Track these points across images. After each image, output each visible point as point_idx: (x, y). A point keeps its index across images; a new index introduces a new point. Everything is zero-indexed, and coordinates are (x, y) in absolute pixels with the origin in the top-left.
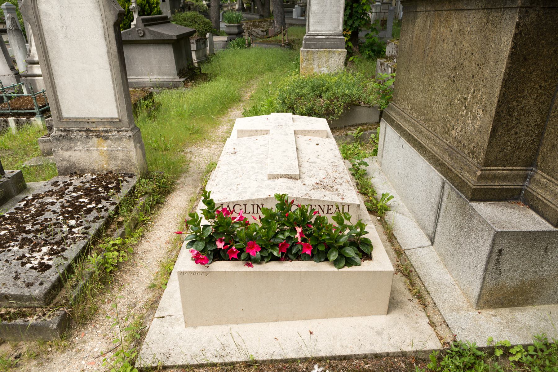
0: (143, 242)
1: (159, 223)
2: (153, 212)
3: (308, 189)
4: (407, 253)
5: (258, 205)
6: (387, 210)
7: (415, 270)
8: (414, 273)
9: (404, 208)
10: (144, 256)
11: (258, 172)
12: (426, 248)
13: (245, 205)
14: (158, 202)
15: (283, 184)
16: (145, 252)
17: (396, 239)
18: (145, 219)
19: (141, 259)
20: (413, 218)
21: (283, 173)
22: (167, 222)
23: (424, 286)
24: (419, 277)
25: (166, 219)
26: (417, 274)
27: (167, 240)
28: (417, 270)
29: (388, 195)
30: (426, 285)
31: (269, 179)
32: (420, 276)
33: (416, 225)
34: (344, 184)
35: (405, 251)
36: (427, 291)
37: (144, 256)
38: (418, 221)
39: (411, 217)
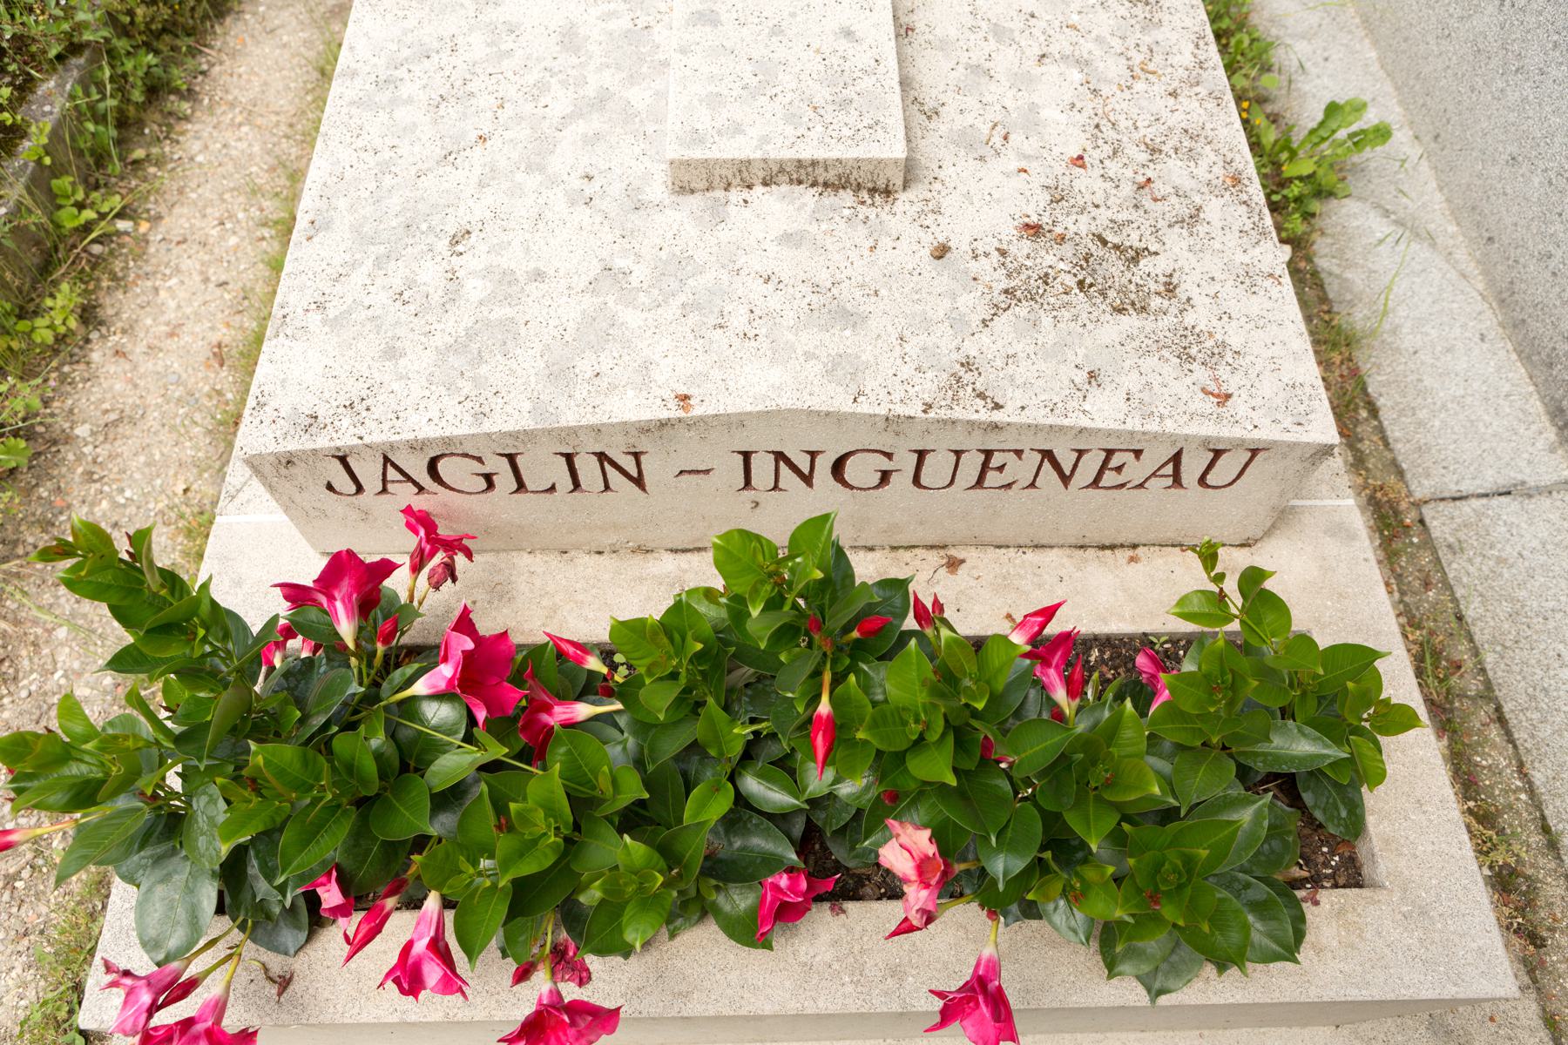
0: (95, 356)
1: (178, 221)
2: (139, 153)
3: (972, 304)
4: (1440, 523)
5: (602, 457)
6: (1331, 194)
7: (1476, 652)
8: (1474, 686)
9: (1426, 197)
10: (103, 452)
11: (602, 100)
12: (1545, 502)
13: (511, 458)
14: (155, 90)
15: (787, 263)
16: (108, 430)
17: (1374, 411)
18: (88, 214)
19: (89, 477)
20: (1472, 268)
21: (782, 151)
22: (215, 212)
23: (1531, 790)
24: (1501, 720)
25: (207, 192)
26: (1488, 692)
27: (215, 338)
28: (1489, 659)
29: (1359, 108)
30: (1538, 778)
31: (684, 189)
32: (1507, 708)
33: (1490, 320)
34: (1214, 209)
35: (1428, 512)
36: (1546, 829)
37: (103, 452)
38: (1505, 298)
39: (1461, 255)
